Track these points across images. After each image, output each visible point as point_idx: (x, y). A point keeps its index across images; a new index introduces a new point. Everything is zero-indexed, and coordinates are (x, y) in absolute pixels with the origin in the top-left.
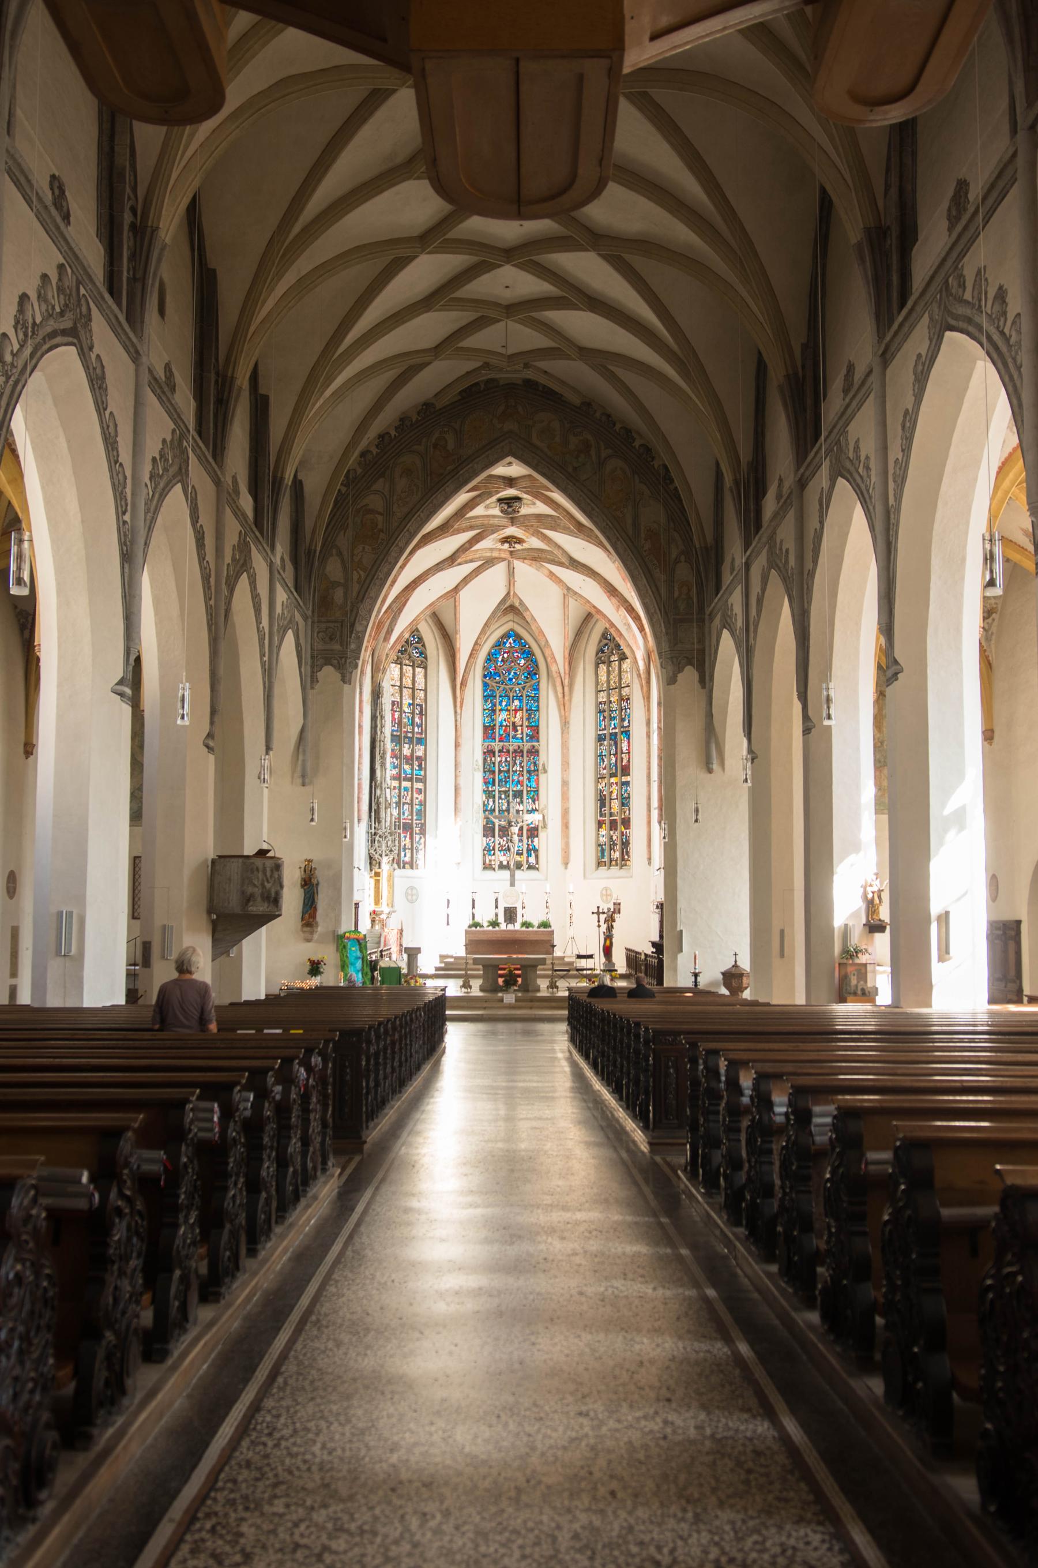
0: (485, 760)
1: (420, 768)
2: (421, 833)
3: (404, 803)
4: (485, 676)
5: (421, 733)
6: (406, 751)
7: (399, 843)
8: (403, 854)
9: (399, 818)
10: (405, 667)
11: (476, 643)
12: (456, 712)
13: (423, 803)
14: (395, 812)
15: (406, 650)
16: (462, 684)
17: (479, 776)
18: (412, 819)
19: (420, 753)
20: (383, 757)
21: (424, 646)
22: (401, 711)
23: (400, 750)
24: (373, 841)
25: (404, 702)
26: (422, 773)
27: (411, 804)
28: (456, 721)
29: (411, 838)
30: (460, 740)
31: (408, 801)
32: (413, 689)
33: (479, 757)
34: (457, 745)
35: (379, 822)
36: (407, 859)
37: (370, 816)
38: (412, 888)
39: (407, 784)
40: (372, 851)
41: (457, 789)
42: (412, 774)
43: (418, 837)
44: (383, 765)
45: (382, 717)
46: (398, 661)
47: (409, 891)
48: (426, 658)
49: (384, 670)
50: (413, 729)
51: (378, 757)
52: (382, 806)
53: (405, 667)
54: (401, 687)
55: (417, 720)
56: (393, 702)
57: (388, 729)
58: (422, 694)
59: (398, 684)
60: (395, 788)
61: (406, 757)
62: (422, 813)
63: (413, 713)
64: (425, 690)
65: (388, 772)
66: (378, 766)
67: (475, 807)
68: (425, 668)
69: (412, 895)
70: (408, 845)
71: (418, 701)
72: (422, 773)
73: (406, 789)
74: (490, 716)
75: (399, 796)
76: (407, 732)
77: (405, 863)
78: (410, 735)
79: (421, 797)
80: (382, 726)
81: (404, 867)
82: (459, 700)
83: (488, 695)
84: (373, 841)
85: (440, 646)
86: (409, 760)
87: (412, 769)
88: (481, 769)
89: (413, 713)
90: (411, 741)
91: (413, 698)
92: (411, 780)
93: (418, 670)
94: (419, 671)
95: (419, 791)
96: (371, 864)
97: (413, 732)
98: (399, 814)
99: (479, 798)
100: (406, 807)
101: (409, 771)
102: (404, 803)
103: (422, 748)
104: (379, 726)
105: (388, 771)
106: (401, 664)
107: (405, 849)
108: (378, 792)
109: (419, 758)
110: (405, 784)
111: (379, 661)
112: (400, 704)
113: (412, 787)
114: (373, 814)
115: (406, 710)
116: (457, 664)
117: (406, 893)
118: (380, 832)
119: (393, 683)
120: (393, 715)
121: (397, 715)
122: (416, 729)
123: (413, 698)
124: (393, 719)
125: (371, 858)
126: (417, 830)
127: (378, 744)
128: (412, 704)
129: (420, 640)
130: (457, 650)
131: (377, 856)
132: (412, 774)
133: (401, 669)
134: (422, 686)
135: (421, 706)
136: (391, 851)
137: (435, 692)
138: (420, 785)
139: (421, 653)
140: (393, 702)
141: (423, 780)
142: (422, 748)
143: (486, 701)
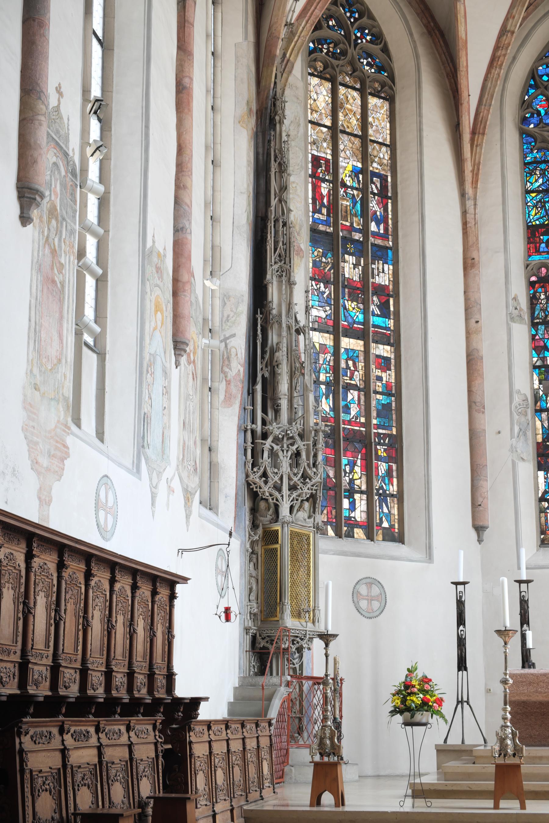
0: (533, 300)
1: (385, 312)
2: (388, 460)
3: (348, 387)
4: (524, 121)
5: (385, 237)
6: (350, 269)
7: (338, 475)
8: (346, 503)
9: (337, 418)
10: (342, 90)
11: (504, 31)
12: (463, 195)
13: (395, 392)
14: (326, 405)
15: (344, 53)
16: (474, 133)
17: (522, 333)
18: (367, 424)
19: (383, 279)
20: (285, 258)
21: (385, 50)
22: (336, 183)
23: (336, 266)
24: (256, 454)
25: (342, 163)
26: (391, 323)
27: (366, 390)
28: (464, 213)
29: (369, 470)
30: (474, 254)
31: (358, 379)
32: (364, 138)
33: (520, 290)
34: (469, 265)
35: (277, 411)
36: (359, 515)
37: (251, 393)
38: (371, 582)
39: (357, 345)
40: (256, 478)
41: (472, 362)
42: (366, 322)
43: (383, 467)
44: (286, 274)
45: (282, 168)
46: (328, 75)
47: (363, 589)
48: (392, 77)
49: (287, 65)
50: (366, 226)
51: (271, 257)
52: (284, 371)
53: (342, 90)
54: (335, 131)
55: (374, 205)
56: (316, 160)
57: (299, 204)
58: (384, 154)
59: (328, 123)
60: (323, 348)
61: (349, 284)
62: (392, 412)
63: (364, 190)
64: (392, 147)
65: (302, 296)
66: (271, 276)
67: (517, 399)
68: (391, 99)
69: (370, 598)
70: (361, 483)
71: (375, 167)
72: (391, 323)
73: (352, 355)
74: (541, 204)
75: (336, 369)
76: (351, 229)
77: (353, 524)
78: (357, 236)
79: (389, 376)
80: (284, 188)
81: (350, 535)
82: (468, 167)
83: (536, 162)
84: (256, 454)
85: (421, 50)
86: (361, 291)
87: (366, 311)
88: (526, 317)
89: (364, 190)
90: (360, 250)
91: (365, 156)
92: (362, 334)
93: (373, 101)
94: (378, 107)
95: (384, 363)
96: (254, 511)
97: (365, 231)
98: (335, 408)
99: (526, 382)
100: (353, 395)
101: (361, 317)
102: (348, 387)
103: (388, 268)
104: (274, 185)
105: (299, 298)
106: (333, 80)
107: (351, 492)
108: (273, 338)
109: (380, 290)
110: (346, 343)
111: (273, 38)
112: (334, 166)
113: (367, 351)
114: (259, 387)
115: (349, 182)
116: (462, 82)
117: (355, 594)
118: (275, 429)
119: (315, 117)
120: (316, 189)
121: (325, 188)
122: (373, 227)
123: (365, 157)
124: (317, 196)
125: (254, 496)
126: (381, 451)
127: (271, 225)
128: (364, 171)
129: (378, 38)
130: (461, 44)
131: (266, 490)
132: (366, 322)
133: (334, 93)
134: (385, 136)
135: (383, 179)
136: (305, 477)
137: (414, 148)
138: (384, 350)
139: (380, 69)
140: (316, 160)
141: (393, 339)
142: (388, 268)
143: (531, 173)
